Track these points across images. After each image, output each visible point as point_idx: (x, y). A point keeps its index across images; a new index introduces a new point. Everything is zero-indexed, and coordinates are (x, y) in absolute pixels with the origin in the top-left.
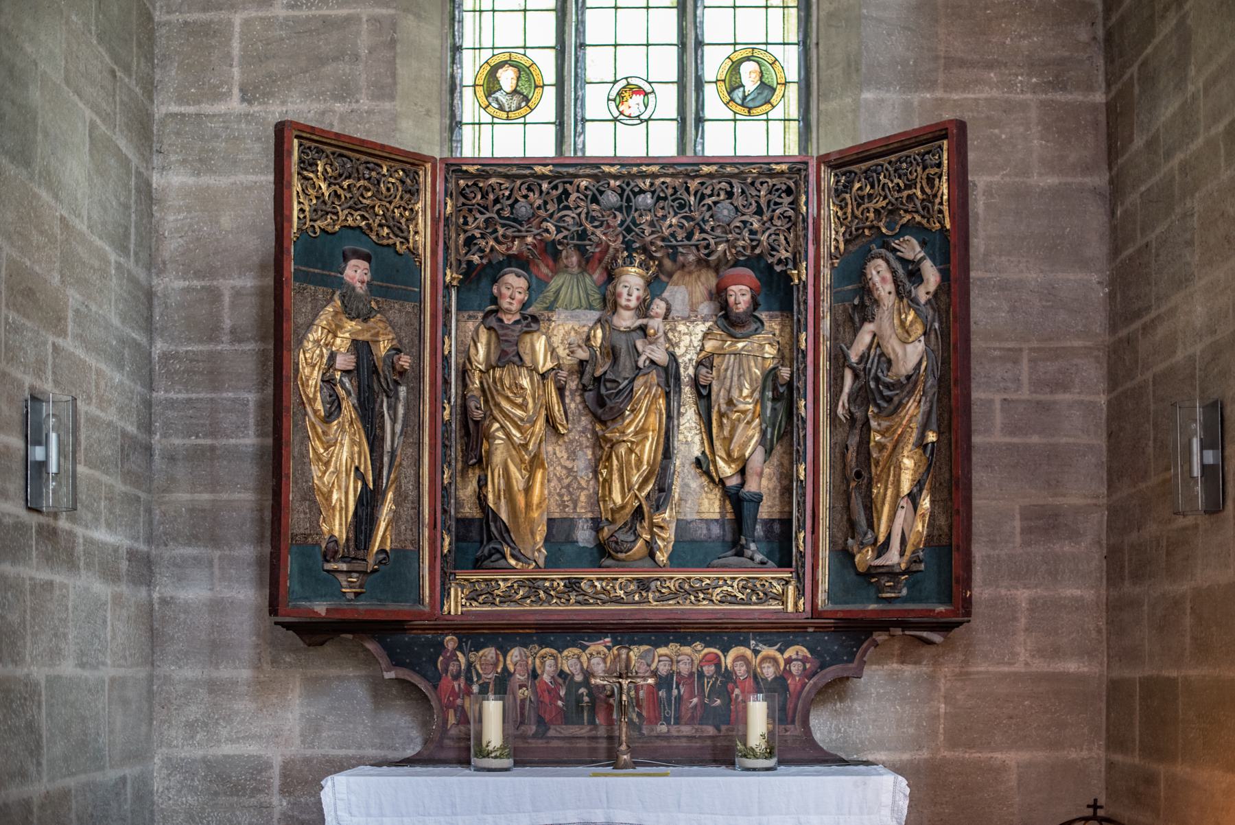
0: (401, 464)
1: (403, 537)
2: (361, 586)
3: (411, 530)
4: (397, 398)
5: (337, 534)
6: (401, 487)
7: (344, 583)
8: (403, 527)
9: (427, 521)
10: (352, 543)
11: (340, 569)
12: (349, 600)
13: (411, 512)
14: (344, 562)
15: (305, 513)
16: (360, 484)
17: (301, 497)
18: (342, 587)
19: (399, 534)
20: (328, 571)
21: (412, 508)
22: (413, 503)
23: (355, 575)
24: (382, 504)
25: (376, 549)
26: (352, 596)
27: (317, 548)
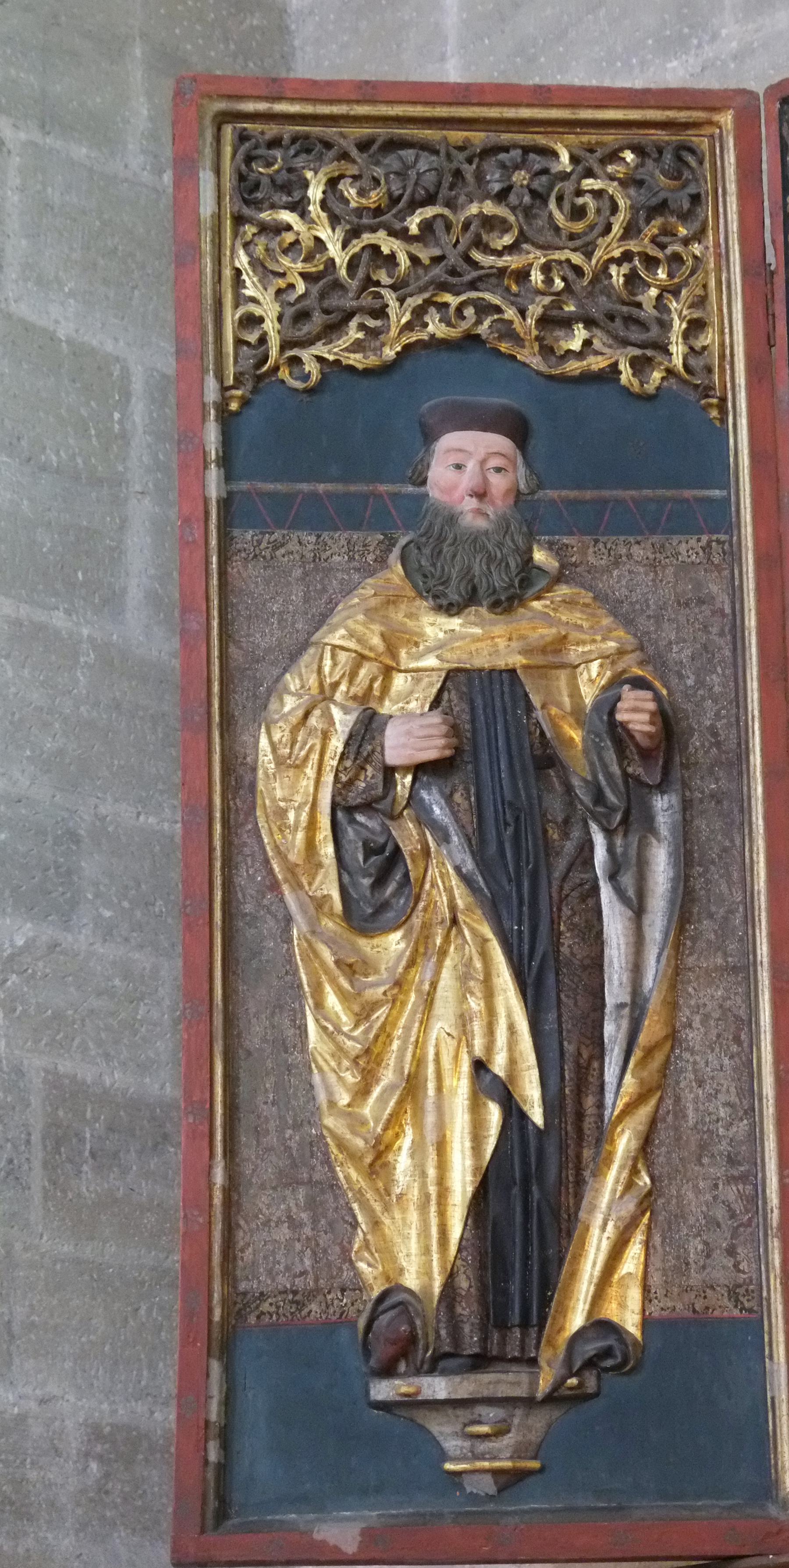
0: (673, 1037)
1: (695, 1278)
2: (518, 1453)
3: (731, 1251)
4: (649, 826)
5: (411, 1281)
6: (680, 1113)
7: (452, 1445)
8: (695, 1246)
9: (775, 1217)
10: (467, 1310)
11: (427, 1394)
12: (474, 1498)
13: (731, 1193)
14: (444, 1373)
15: (294, 1224)
16: (494, 1113)
17: (281, 1173)
18: (444, 1456)
19: (683, 1266)
20: (385, 1406)
21: (731, 1180)
22: (732, 1161)
23: (492, 1413)
24: (599, 1173)
25: (577, 1320)
26: (487, 1485)
27: (344, 1335)
